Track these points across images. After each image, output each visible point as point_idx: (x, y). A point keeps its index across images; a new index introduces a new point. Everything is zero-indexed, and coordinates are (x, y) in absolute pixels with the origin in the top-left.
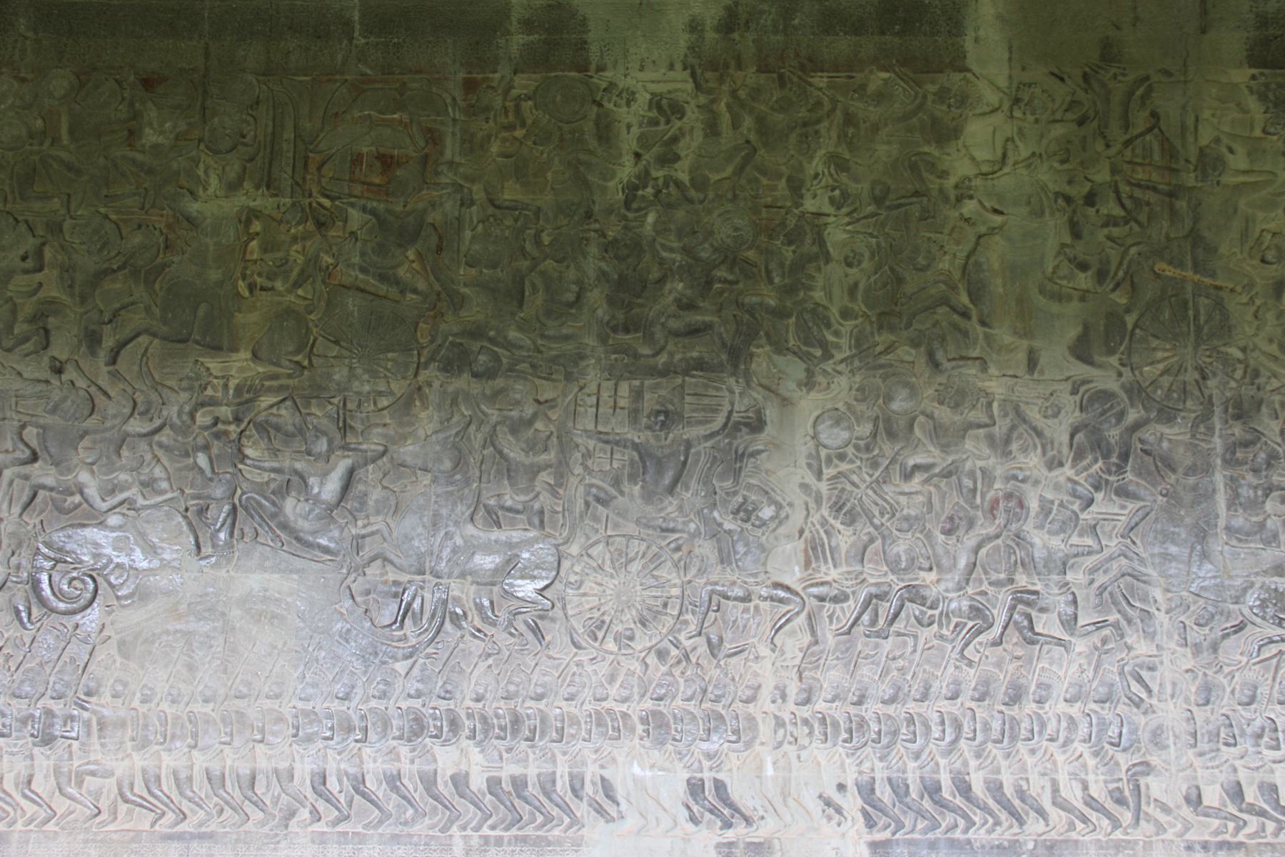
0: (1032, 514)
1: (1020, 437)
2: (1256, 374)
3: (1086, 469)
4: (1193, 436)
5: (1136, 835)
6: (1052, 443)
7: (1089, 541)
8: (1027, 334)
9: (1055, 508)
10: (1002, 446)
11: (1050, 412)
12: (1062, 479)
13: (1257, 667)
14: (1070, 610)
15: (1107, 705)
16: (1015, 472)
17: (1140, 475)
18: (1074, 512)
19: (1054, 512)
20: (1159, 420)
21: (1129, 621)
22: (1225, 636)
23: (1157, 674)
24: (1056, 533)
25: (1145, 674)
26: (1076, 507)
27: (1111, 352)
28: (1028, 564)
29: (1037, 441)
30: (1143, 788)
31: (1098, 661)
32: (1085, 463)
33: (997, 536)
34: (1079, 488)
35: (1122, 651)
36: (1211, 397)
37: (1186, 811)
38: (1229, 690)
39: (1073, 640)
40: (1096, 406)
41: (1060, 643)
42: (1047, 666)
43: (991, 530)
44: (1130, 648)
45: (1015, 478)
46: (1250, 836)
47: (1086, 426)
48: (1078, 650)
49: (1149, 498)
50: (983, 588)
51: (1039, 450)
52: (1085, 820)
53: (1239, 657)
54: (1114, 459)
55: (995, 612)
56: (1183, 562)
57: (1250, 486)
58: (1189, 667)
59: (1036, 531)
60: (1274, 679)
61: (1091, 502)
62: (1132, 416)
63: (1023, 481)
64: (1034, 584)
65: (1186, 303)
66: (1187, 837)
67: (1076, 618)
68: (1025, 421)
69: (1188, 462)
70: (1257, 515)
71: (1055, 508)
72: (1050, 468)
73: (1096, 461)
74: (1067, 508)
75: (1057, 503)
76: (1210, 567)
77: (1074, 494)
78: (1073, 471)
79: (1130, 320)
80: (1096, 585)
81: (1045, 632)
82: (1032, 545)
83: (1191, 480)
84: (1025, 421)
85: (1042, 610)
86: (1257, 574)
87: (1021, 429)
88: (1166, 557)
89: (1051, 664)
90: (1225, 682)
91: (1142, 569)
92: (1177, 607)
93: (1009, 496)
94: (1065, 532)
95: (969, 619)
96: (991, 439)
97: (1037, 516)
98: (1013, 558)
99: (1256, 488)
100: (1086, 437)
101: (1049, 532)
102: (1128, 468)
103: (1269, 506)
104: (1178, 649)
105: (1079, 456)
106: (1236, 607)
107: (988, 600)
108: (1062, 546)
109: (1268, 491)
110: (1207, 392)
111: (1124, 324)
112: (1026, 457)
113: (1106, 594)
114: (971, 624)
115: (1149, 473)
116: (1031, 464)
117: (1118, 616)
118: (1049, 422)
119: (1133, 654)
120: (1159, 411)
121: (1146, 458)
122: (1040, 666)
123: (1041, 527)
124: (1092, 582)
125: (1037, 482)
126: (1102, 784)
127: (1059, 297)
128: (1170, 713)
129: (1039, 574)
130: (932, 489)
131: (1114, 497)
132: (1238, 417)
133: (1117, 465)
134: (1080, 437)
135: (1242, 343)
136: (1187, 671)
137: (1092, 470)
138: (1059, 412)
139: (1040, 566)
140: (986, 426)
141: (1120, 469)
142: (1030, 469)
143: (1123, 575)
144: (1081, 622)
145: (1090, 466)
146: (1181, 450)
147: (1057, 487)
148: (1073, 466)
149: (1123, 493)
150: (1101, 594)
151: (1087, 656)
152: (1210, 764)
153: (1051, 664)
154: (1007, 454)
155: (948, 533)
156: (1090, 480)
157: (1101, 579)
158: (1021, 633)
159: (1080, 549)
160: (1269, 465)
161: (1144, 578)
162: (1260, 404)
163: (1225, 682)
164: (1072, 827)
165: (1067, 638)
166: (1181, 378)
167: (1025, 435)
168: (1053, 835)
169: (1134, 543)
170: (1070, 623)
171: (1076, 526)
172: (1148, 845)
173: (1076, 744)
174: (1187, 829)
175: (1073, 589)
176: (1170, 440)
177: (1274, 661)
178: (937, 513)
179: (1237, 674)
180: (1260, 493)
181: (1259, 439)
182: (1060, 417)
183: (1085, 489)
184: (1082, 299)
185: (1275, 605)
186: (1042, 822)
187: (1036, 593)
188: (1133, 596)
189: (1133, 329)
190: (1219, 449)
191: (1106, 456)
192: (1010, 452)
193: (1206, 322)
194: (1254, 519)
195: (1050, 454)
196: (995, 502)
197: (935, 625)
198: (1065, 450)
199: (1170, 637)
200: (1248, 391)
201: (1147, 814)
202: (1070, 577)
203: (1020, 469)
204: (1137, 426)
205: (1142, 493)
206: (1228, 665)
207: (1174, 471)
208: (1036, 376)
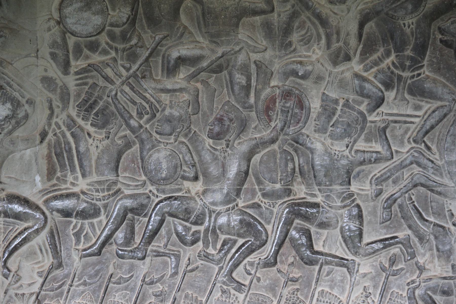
0: (313, 115)
1: (302, 26)
3: (376, 64)
6: (338, 33)
7: (378, 147)
9: (339, 108)
10: (281, 37)
12: (348, 75)
14: (353, 226)
16: (294, 66)
17: (438, 70)
18: (361, 113)
19: (338, 112)
21: (421, 239)
24: (341, 137)
26: (363, 108)
28: (307, 173)
29: (321, 30)
31: (385, 284)
32: (375, 56)
33: (273, 141)
34: (367, 85)
35: (412, 273)
39: (357, 260)
41: (342, 262)
42: (327, 289)
43: (266, 134)
44: (421, 269)
45: (295, 73)
47: (378, 13)
48: (361, 271)
50: (256, 200)
51: (323, 41)
54: (409, 52)
55: (269, 228)
59: (317, 135)
61: (380, 101)
63: (304, 77)
64: (315, 196)
67: (361, 235)
68: (308, 8)
71: (339, 108)
72: (335, 63)
73: (388, 54)
74: (353, 109)
75: (341, 102)
77: (362, 93)
78: (361, 67)
80: (385, 196)
81: (326, 250)
82: (312, 151)
84: (308, 8)
85: (323, 225)
87: (303, 17)
89: (332, 288)
91: (437, 178)
93: (287, 95)
94: (350, 136)
95: (239, 235)
96: (268, 28)
97: (318, 117)
98: (290, 165)
100: (377, 25)
101: (331, 136)
102: (425, 62)
105: (369, 48)
107: (261, 214)
108: (347, 153)
112: (308, 50)
113: (395, 207)
114: (241, 241)
116: (314, 57)
117: (409, 232)
119: (425, 275)
121: (447, 51)
122: (319, 289)
123: (322, 130)
124: (380, 193)
125: (319, 79)
129: (319, 184)
130: (199, 85)
131: (407, 96)
133: (412, 59)
134: (370, 26)
137: (383, 65)
139: (321, 175)
140: (263, 12)
141: (416, 64)
142: (312, 63)
143: (415, 186)
144: (366, 239)
145: (381, 60)
147: (342, 85)
148: (362, 61)
149: (418, 91)
150: (390, 207)
151: (373, 279)
153: (332, 288)
154: (286, 46)
155: (216, 137)
156: (380, 76)
157: (390, 190)
158: (298, 251)
159: (367, 156)
161: (439, 189)
165: (350, 257)
167: (308, 24)
169: (429, 148)
170: (353, 240)
171: (363, 129)
175: (358, 201)
178: (204, 114)
183: (374, 87)
187: (316, 205)
188: (426, 210)
191: (399, 49)
192: (290, 44)
195: (335, 45)
196: (273, 100)
197: (200, 243)
198: (353, 41)
202: (354, 187)
203: (301, 63)
205: (440, 90)
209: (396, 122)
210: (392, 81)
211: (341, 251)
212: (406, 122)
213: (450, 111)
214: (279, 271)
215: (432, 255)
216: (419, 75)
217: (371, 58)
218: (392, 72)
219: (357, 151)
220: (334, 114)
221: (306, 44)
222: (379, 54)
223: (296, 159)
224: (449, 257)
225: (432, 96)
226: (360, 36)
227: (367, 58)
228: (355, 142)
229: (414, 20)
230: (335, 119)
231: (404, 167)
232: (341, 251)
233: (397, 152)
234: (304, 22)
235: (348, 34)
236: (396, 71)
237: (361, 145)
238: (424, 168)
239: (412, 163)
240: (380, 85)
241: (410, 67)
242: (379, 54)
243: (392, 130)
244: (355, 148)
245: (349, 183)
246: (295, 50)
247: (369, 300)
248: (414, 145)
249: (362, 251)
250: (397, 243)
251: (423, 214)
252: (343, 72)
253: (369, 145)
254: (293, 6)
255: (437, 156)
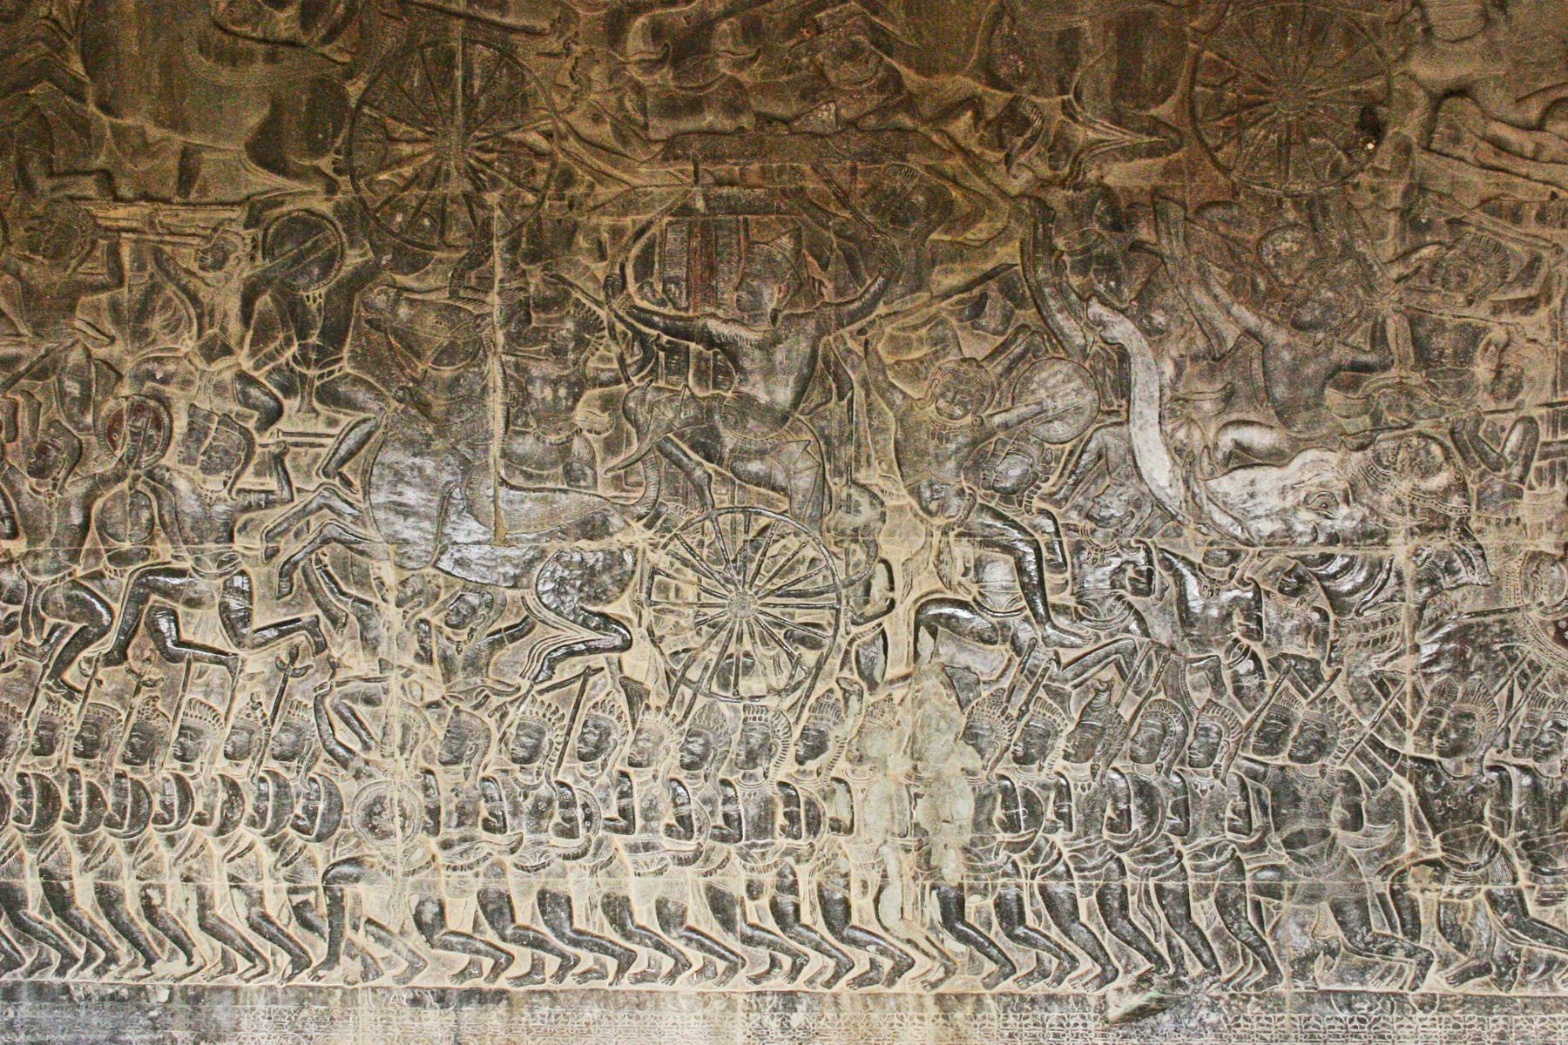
2: (568, 179)
4: (453, 294)
5: (333, 977)
6: (212, 315)
7: (271, 483)
8: (178, 123)
9: (214, 426)
10: (135, 321)
11: (210, 260)
12: (228, 376)
13: (547, 697)
15: (295, 763)
16: (149, 366)
18: (245, 432)
19: (212, 433)
20: (396, 267)
22: (497, 644)
23: (381, 709)
25: (362, 710)
26: (251, 425)
27: (318, 150)
28: (171, 525)
30: (348, 903)
33: (119, 478)
34: (254, 392)
36: (487, 223)
37: (416, 939)
38: (496, 736)
39: (242, 654)
40: (288, 247)
46: (519, 980)
48: (248, 670)
49: (375, 406)
50: (101, 567)
51: (195, 327)
52: (250, 954)
53: (519, 680)
54: (314, 339)
56: (427, 517)
57: (546, 380)
58: (437, 697)
59: (183, 468)
60: (573, 719)
62: (354, 259)
63: (165, 381)
65: (451, 55)
66: (417, 981)
69: (443, 339)
70: (558, 431)
72: (210, 359)
73: (288, 342)
76: (474, 525)
77: (245, 400)
78: (251, 363)
79: (354, 89)
81: (198, 640)
83: (447, 372)
85: (193, 603)
86: (551, 535)
88: (403, 510)
89: (207, 695)
90: (492, 723)
91: (360, 530)
92: (414, 594)
94: (229, 468)
95: (72, 619)
98: (145, 515)
99: (555, 383)
100: (274, 300)
102: (346, 353)
103: (580, 415)
104: (419, 666)
105: (262, 335)
106: (517, 593)
107: (103, 588)
108: (225, 493)
109: (578, 387)
110: (480, 213)
111: (344, 98)
114: (76, 627)
115: (379, 362)
117: (319, 612)
118: (210, 276)
120: (398, 251)
121: (376, 336)
123: (189, 460)
125: (186, 383)
126: (284, 895)
127: (234, 59)
128: (396, 779)
129: (186, 542)
130: (20, 399)
131: (316, 404)
132: (533, 257)
134: (264, 302)
135: (546, 125)
136: (429, 706)
138: (225, 259)
140: (104, 288)
141: (326, 356)
144: (257, 622)
145: (279, 352)
146: (431, 319)
147: (220, 389)
148: (253, 354)
149: (329, 396)
152: (459, 863)
153: (207, 695)
154: (141, 336)
155: (39, 472)
157: (290, 548)
159: (253, 498)
160: (581, 343)
161: (360, 547)
162: (568, 234)
163: (492, 723)
164: (228, 966)
166: (439, 191)
168: (199, 980)
169: (348, 483)
170: (233, 624)
172: (349, 996)
173: (242, 828)
174: (414, 969)
175: (244, 566)
176: (412, 302)
177: (578, 685)
178: (25, 442)
179: (512, 710)
180: (562, 392)
181: (567, 295)
182: (228, 267)
184: (271, 58)
185: (580, 590)
186: (182, 957)
187: (181, 573)
188: (345, 578)
189: (359, 107)
190: (497, 317)
193: (483, 90)
194: (553, 438)
196: (117, 418)
197: (19, 631)
198: (235, 327)
199: (402, 646)
200: (551, 209)
201: (351, 944)
202: (239, 543)
204: (362, 278)
205: (361, 395)
206: (499, 693)
207: (418, 356)
208: (193, 196)
209: (296, 445)
210: (293, 384)
211: (220, 641)
212: (312, 445)
213: (377, 427)
214: (130, 671)
215: (355, 645)
216: (331, 373)
217: (266, 350)
218: (292, 370)
219: (239, 491)
220: (206, 435)
221: (172, 332)
222: (278, 342)
223: (155, 504)
224: (375, 648)
225: (351, 404)
226: (246, 317)
227: (260, 350)
228: (237, 476)
229: (323, 291)
230: (207, 443)
231: (311, 513)
232: (220, 641)
233: (299, 490)
234: (170, 300)
235: (226, 315)
236: (298, 369)
237: (248, 480)
238: (339, 515)
239: (320, 508)
240: (275, 391)
241: (317, 361)
242: (278, 342)
243: (294, 459)
244: (238, 485)
245: (231, 539)
246: (154, 341)
247: (259, 714)
248: (324, 479)
249: (247, 641)
250: (300, 628)
251: (341, 584)
252: (220, 372)
253: (262, 480)
254: (152, 276)
255: (360, 496)
